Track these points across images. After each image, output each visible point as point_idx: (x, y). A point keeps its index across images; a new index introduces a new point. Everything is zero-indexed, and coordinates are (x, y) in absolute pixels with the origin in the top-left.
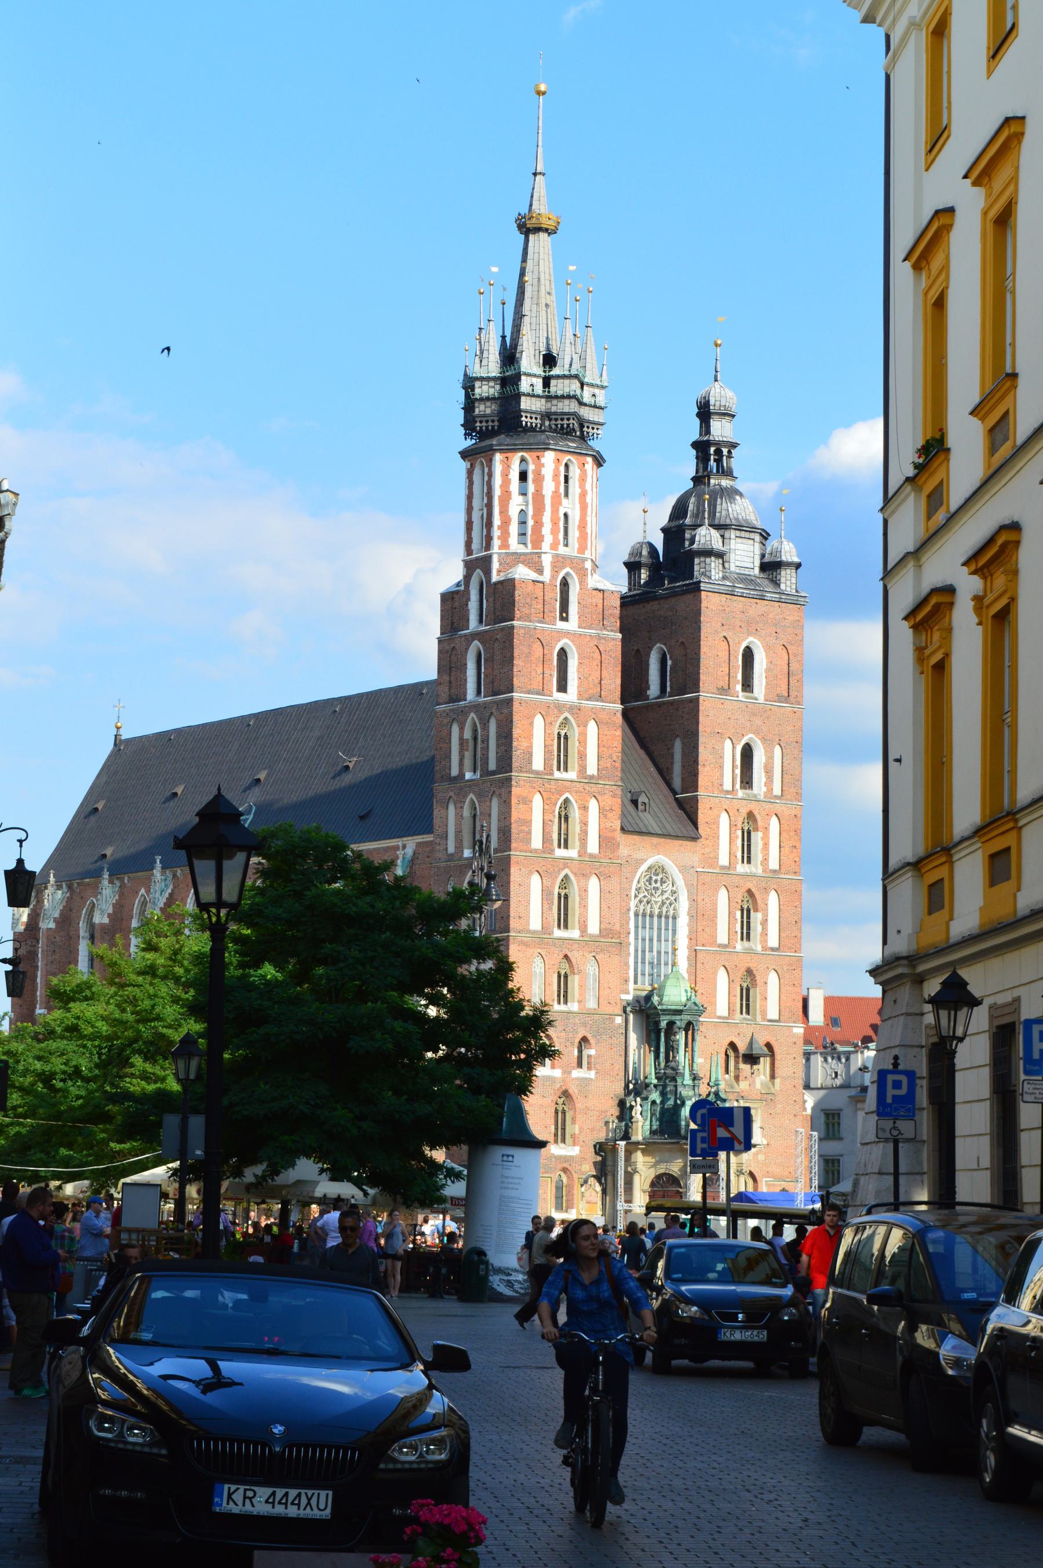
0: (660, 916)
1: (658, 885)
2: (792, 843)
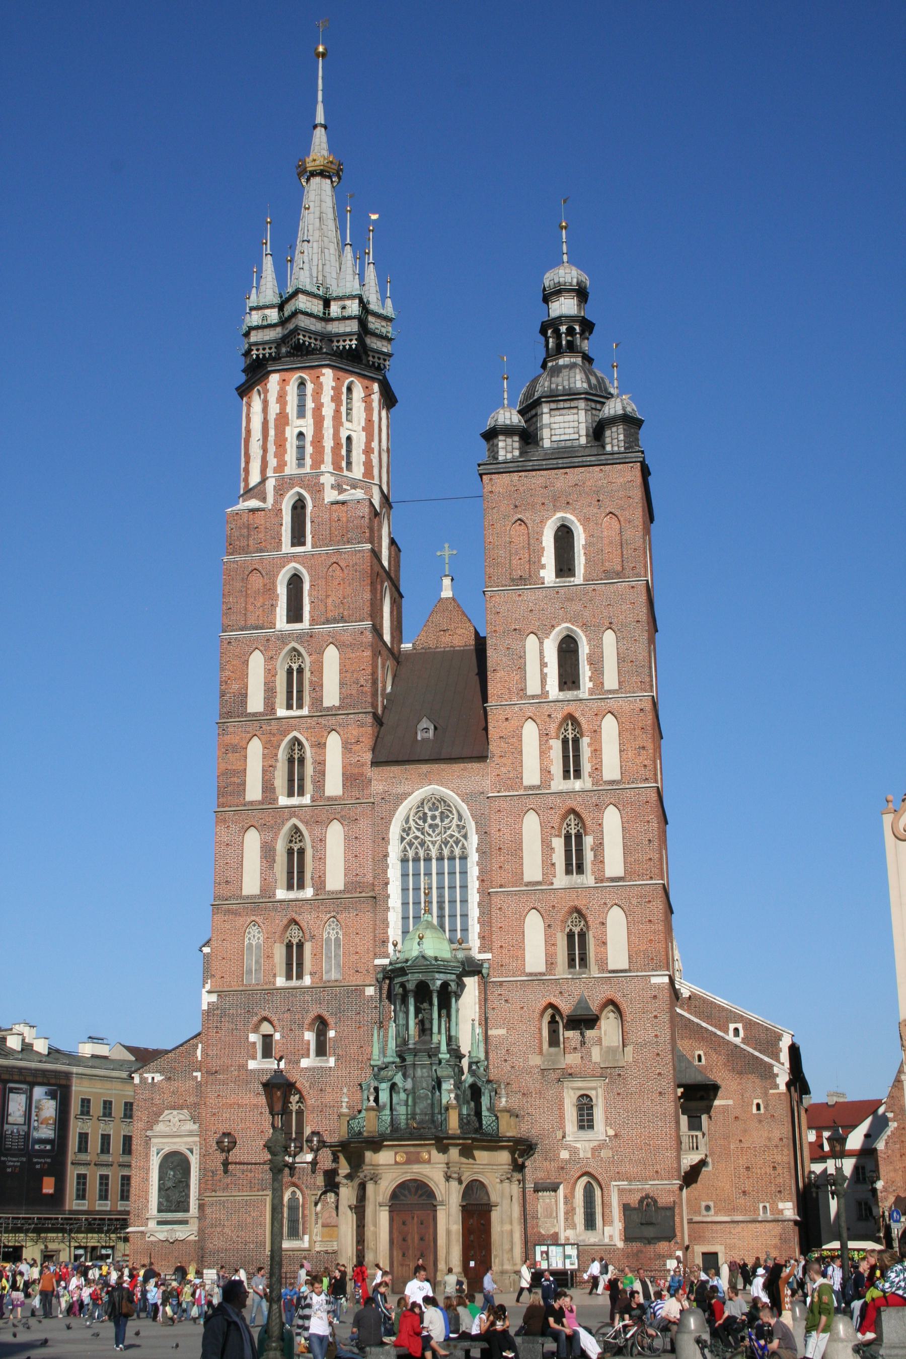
0: (440, 859)
1: (438, 821)
2: (639, 743)
